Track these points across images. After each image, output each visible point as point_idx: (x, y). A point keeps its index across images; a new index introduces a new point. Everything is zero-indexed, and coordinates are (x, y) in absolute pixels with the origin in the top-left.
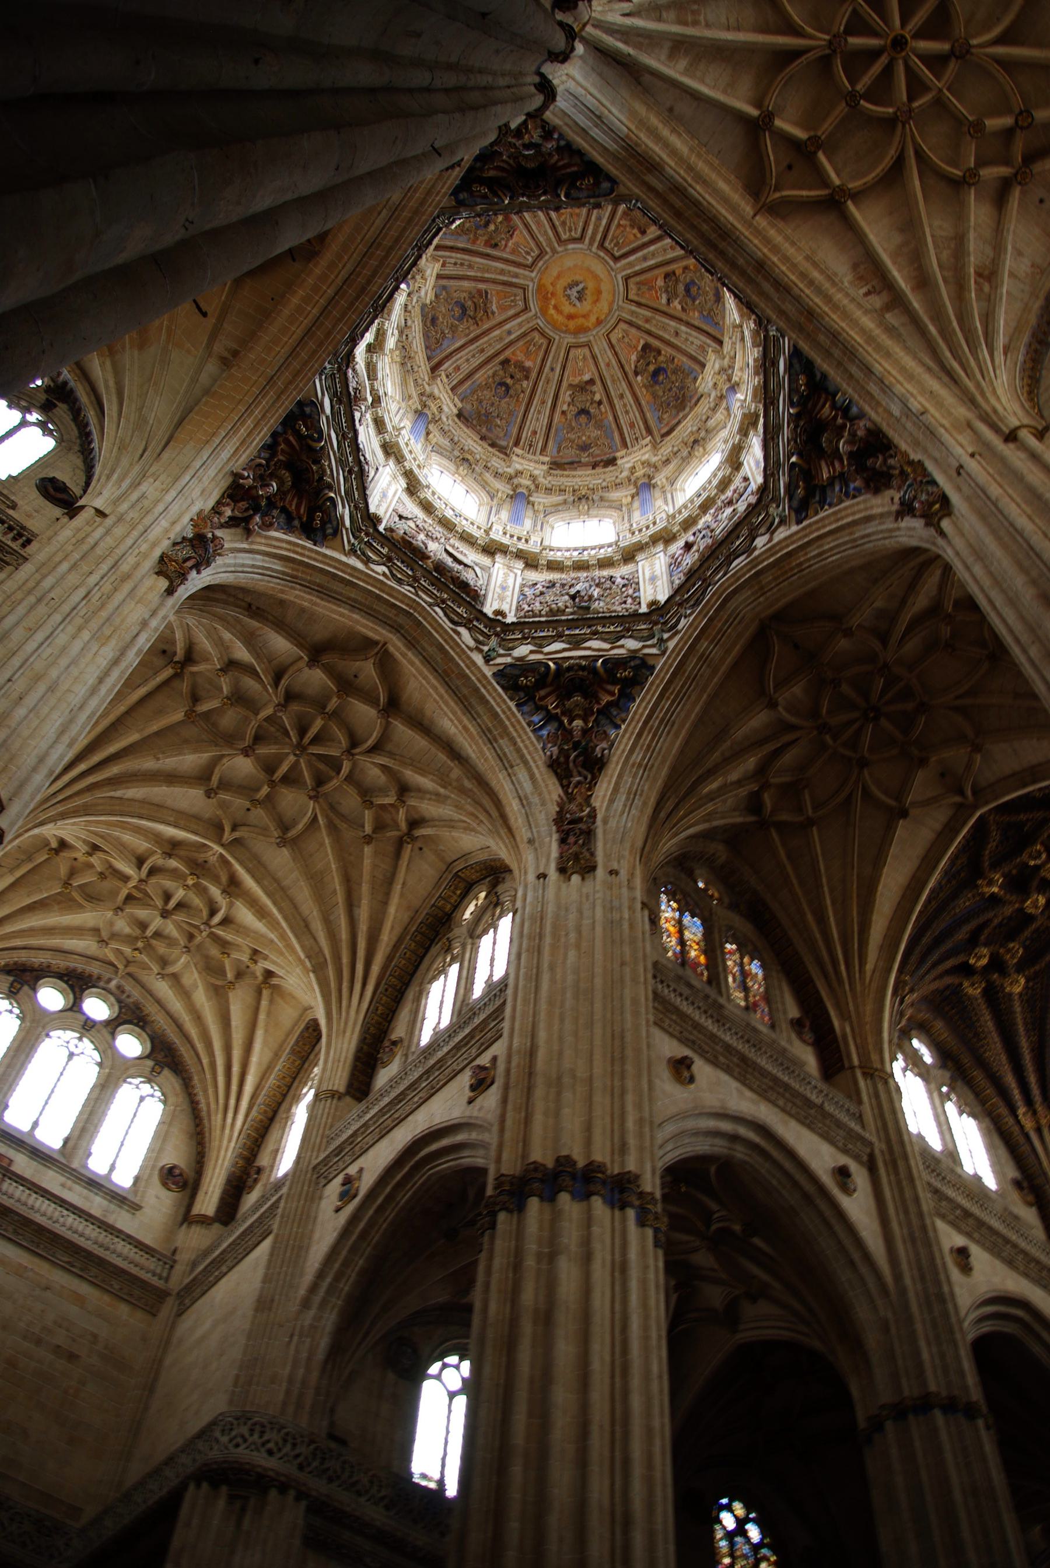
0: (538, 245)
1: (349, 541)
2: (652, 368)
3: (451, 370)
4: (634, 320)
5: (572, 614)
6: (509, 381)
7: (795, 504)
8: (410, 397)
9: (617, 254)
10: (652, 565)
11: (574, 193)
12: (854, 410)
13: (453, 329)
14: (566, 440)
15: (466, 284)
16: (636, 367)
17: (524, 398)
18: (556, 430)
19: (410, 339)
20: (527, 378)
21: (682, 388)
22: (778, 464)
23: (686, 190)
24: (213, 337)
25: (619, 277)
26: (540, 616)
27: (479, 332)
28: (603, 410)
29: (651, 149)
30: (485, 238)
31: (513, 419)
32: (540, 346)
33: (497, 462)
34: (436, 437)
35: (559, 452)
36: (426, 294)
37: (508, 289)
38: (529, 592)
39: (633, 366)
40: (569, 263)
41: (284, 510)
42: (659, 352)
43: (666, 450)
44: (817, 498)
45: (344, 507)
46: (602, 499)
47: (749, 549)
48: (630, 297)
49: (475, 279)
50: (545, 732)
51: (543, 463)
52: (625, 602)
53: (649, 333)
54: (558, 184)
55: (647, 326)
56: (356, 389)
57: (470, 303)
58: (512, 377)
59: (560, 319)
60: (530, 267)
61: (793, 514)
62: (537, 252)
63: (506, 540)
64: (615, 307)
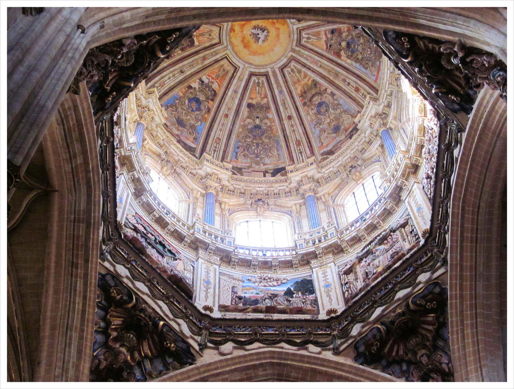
0: (305, 47)
4: (212, 51)
7: (108, 278)
11: (375, 331)
22: (135, 278)
25: (241, 66)
30: (344, 35)
44: (103, 302)
48: (225, 59)
53: (197, 53)
54: (388, 331)
55: (201, 55)
60: (300, 31)
61: (103, 272)
62: (303, 42)
64: (229, 47)
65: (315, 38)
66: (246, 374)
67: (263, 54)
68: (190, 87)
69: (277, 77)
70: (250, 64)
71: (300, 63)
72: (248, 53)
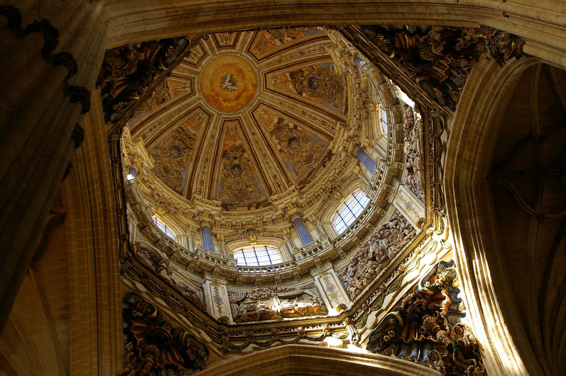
0: (186, 78)
1: (219, 349)
2: (305, 83)
3: (199, 186)
4: (272, 67)
5: (381, 269)
6: (236, 162)
7: (442, 102)
8: (188, 226)
9: (231, 44)
10: (401, 198)
11: (169, 61)
12: (423, 27)
13: (180, 163)
14: (295, 164)
15: (166, 134)
16: (297, 90)
17: (252, 163)
18: (286, 164)
19: (161, 195)
20: (244, 151)
21: (332, 78)
23: (224, 7)
24: (47, 310)
25: (244, 53)
26: (365, 287)
27: (195, 152)
28: (301, 129)
29: (186, 6)
31: (257, 180)
32: (236, 128)
33: (268, 215)
34: (221, 233)
35: (297, 175)
36: (148, 163)
37: (191, 115)
38: (347, 278)
39: (295, 92)
40: (211, 72)
41: (167, 367)
42: (302, 71)
43: (353, 122)
44: (451, 88)
45: (199, 333)
46: (343, 181)
47: (443, 147)
48: (259, 59)
49: (168, 127)
50: (426, 357)
51: (294, 191)
52: (405, 235)
53: (287, 66)
54: (156, 64)
55: (282, 64)
56: (152, 257)
57: (177, 142)
58: (235, 158)
59: (233, 104)
60: (192, 93)
61: (446, 108)
63: (309, 259)
65: (178, 90)
66: (304, 11)
67: (224, 65)
68: (293, 38)
69: (210, 48)
70: (236, 56)
71: (189, 63)
72: (238, 65)
